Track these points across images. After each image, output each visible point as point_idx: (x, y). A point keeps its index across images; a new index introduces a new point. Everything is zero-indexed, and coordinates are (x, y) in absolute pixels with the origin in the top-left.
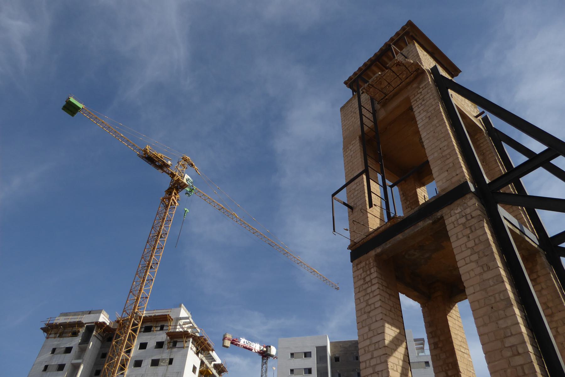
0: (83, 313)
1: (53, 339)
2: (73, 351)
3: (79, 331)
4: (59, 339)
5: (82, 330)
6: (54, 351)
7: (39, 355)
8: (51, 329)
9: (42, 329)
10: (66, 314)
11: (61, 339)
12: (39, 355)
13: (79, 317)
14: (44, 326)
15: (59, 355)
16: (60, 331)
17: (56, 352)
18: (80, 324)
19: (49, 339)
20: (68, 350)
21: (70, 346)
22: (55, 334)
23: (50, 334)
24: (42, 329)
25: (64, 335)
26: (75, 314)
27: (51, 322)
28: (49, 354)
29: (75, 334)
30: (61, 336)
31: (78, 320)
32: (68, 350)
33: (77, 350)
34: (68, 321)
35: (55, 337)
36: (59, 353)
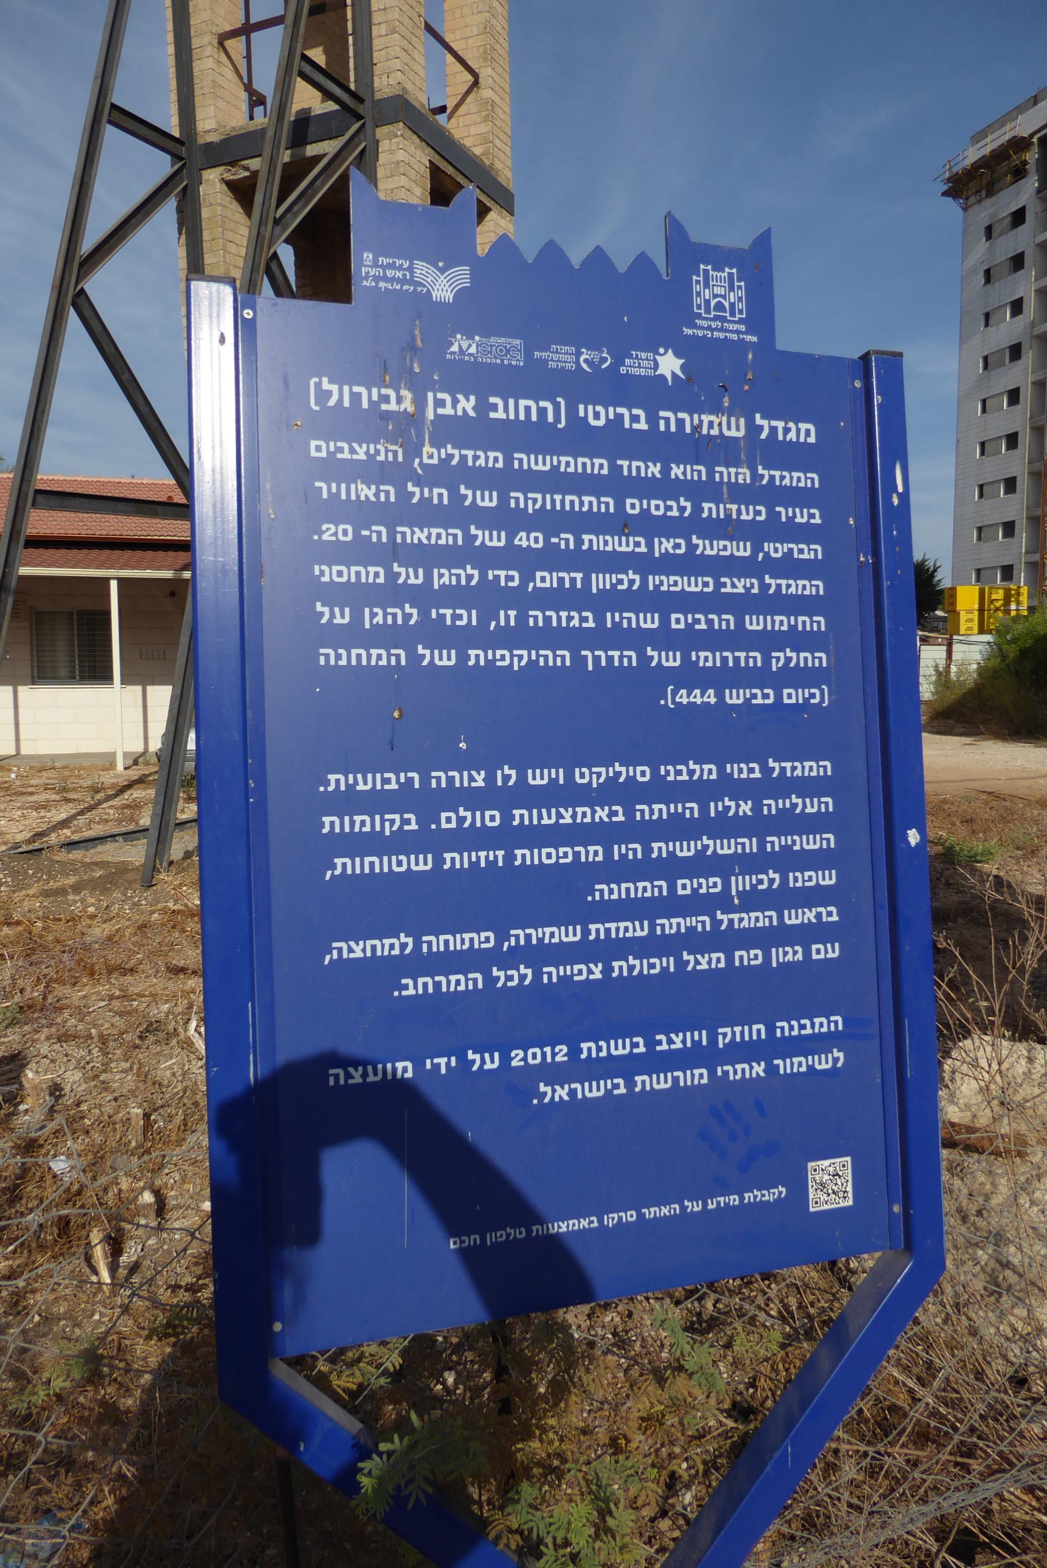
0: (1021, 109)
1: (977, 207)
2: (1029, 216)
3: (1025, 163)
4: (988, 202)
5: (1032, 156)
6: (989, 231)
7: (965, 254)
8: (967, 185)
9: (944, 194)
10: (982, 135)
11: (994, 198)
12: (965, 254)
13: (1008, 127)
14: (946, 187)
15: (1004, 237)
16: (984, 182)
17: (996, 231)
18: (1019, 144)
19: (970, 210)
20: (1018, 217)
21: (1020, 206)
22: (977, 192)
23: (967, 199)
24: (944, 194)
25: (997, 186)
26: (1002, 122)
27: (955, 170)
28: (983, 245)
29: (1019, 173)
30: (991, 190)
31: (1007, 137)
32: (1018, 217)
33: (1039, 210)
34: (987, 150)
35: (980, 201)
36: (1001, 234)
